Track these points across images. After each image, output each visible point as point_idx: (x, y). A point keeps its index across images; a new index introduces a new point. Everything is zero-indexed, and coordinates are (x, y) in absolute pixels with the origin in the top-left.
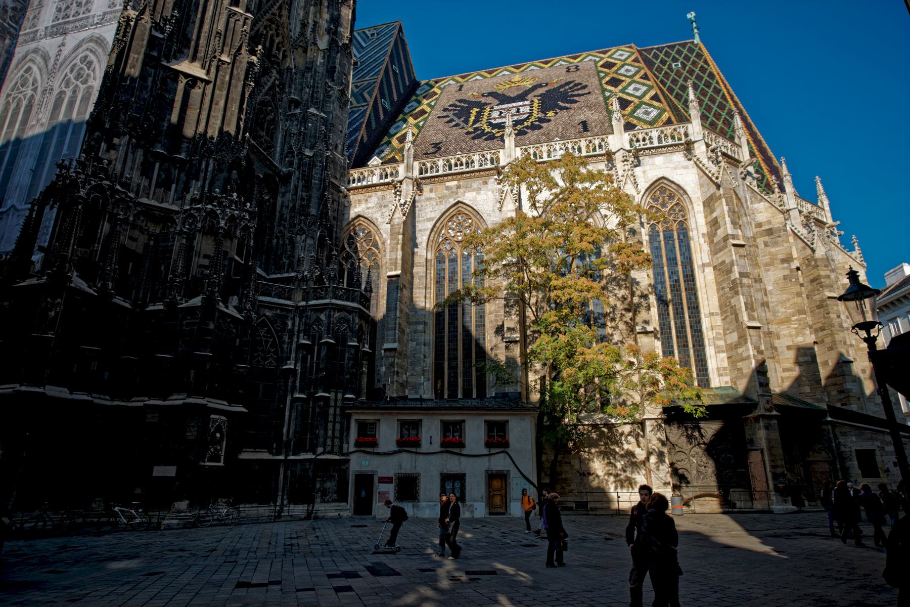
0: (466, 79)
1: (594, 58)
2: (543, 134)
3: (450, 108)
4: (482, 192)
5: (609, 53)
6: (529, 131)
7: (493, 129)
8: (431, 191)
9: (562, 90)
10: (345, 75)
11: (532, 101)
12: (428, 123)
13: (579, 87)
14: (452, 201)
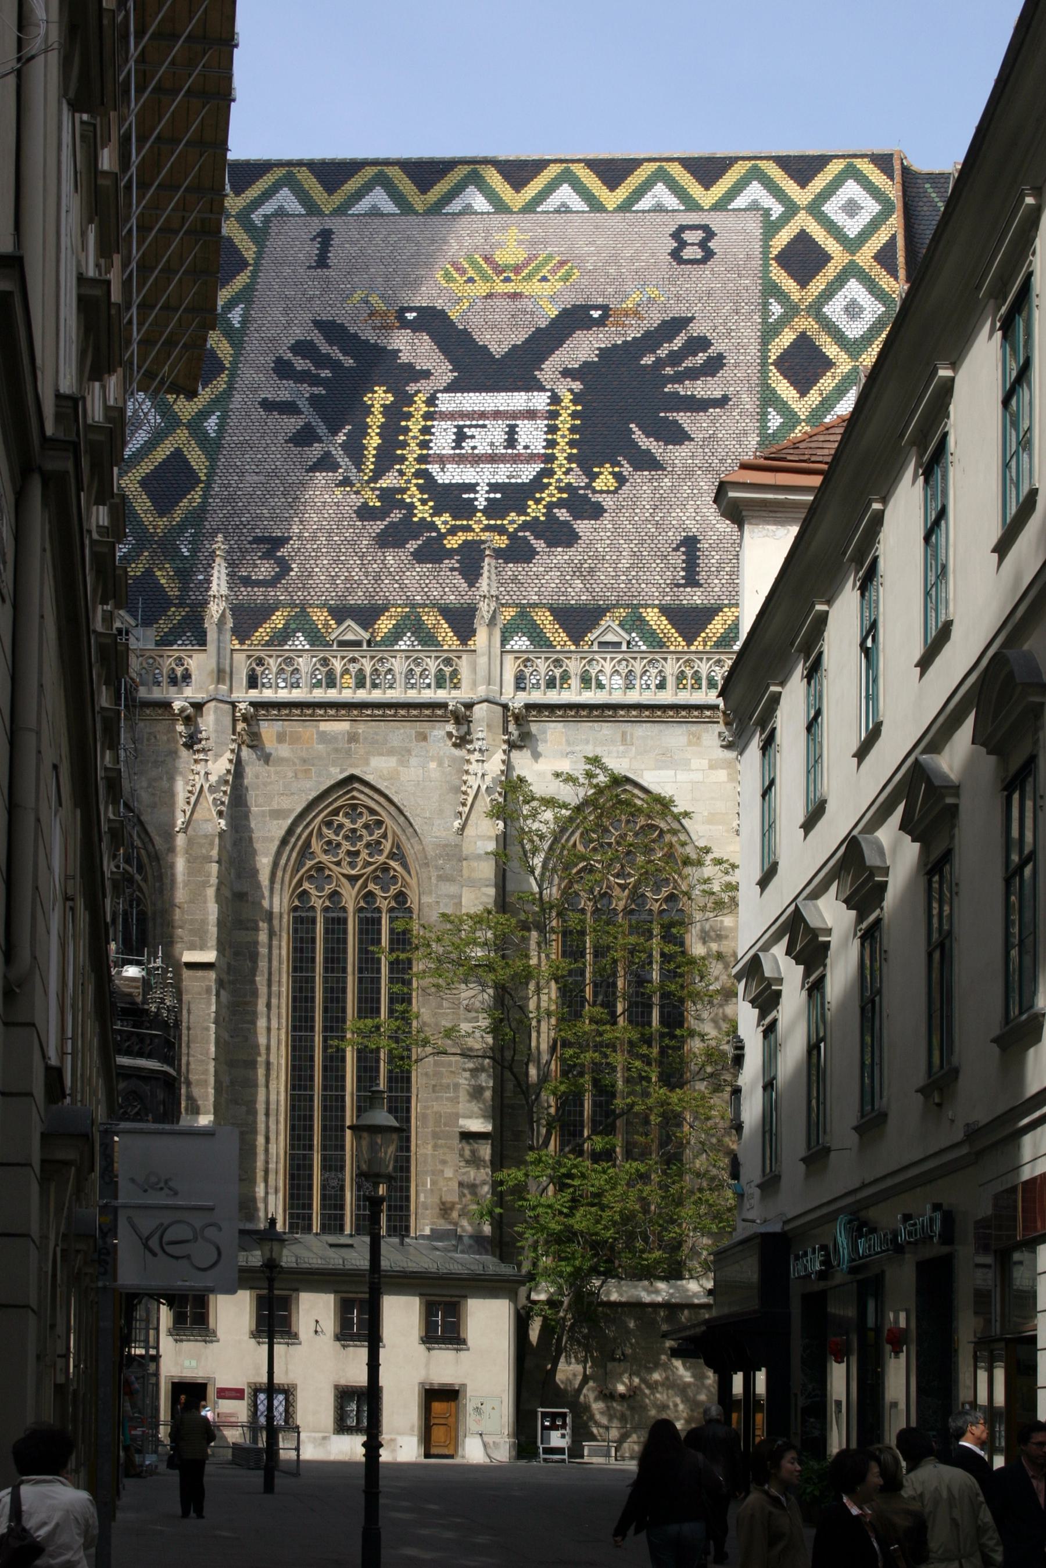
0: (338, 198)
1: (768, 201)
2: (577, 570)
3: (301, 364)
4: (413, 761)
5: (819, 183)
6: (539, 545)
7: (437, 512)
9: (648, 360)
11: (555, 399)
13: (701, 358)
14: (337, 774)
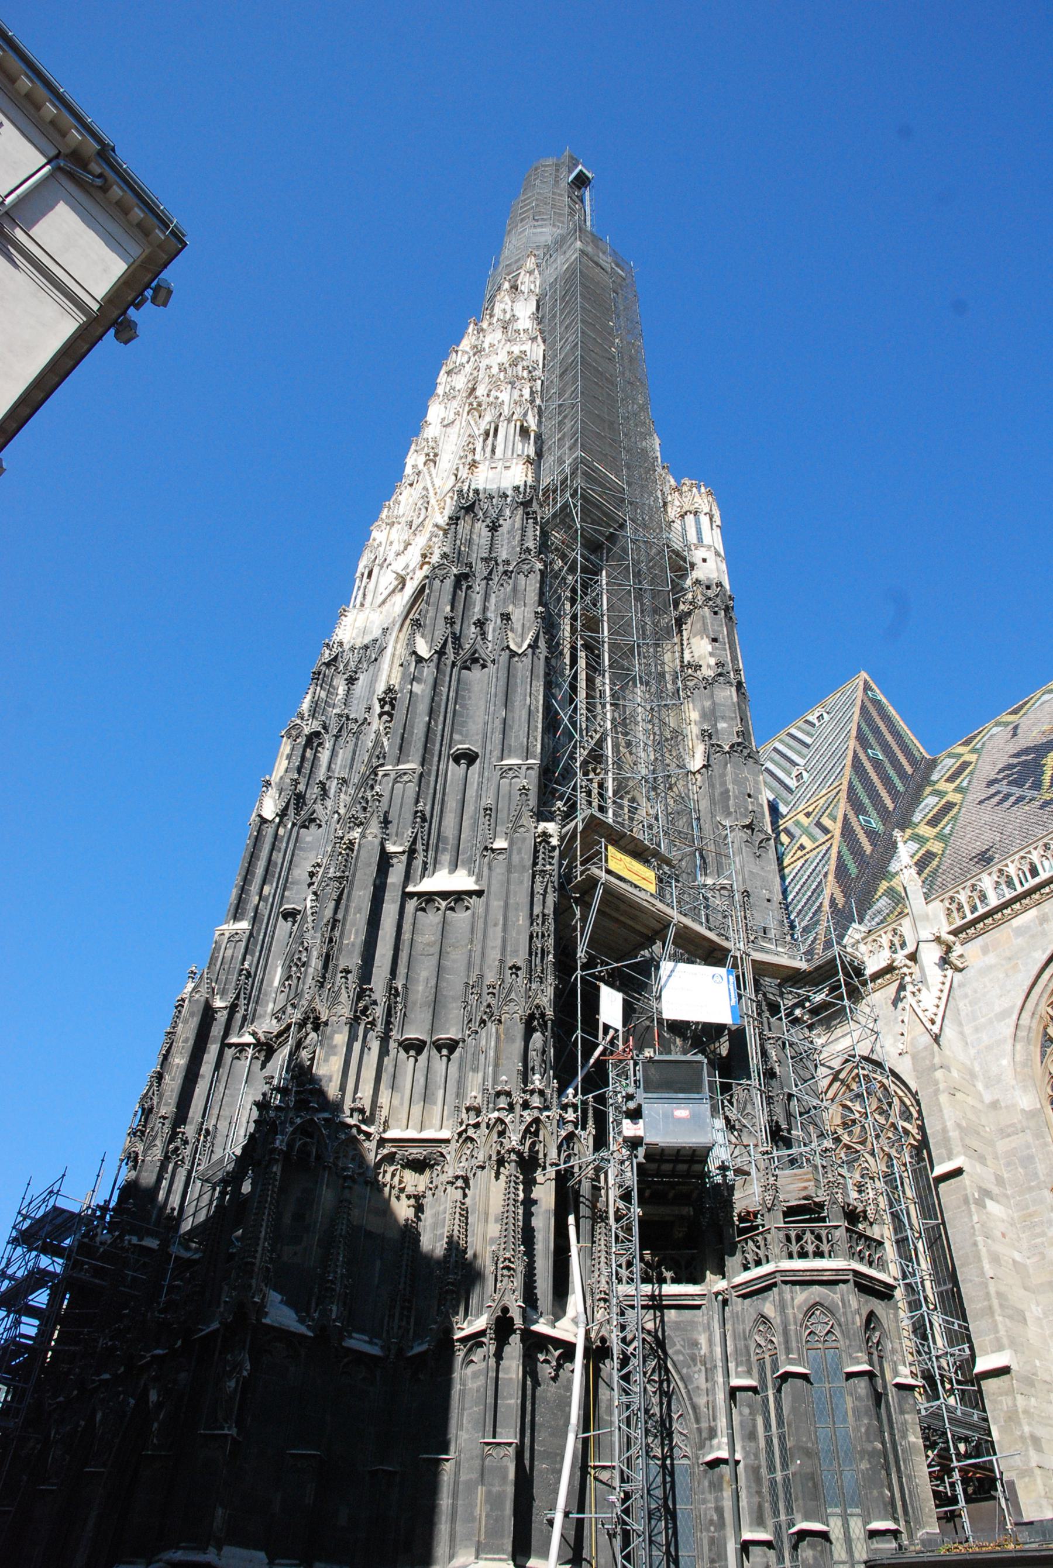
0: (1022, 713)
8: (985, 950)
10: (749, 796)
12: (961, 821)
